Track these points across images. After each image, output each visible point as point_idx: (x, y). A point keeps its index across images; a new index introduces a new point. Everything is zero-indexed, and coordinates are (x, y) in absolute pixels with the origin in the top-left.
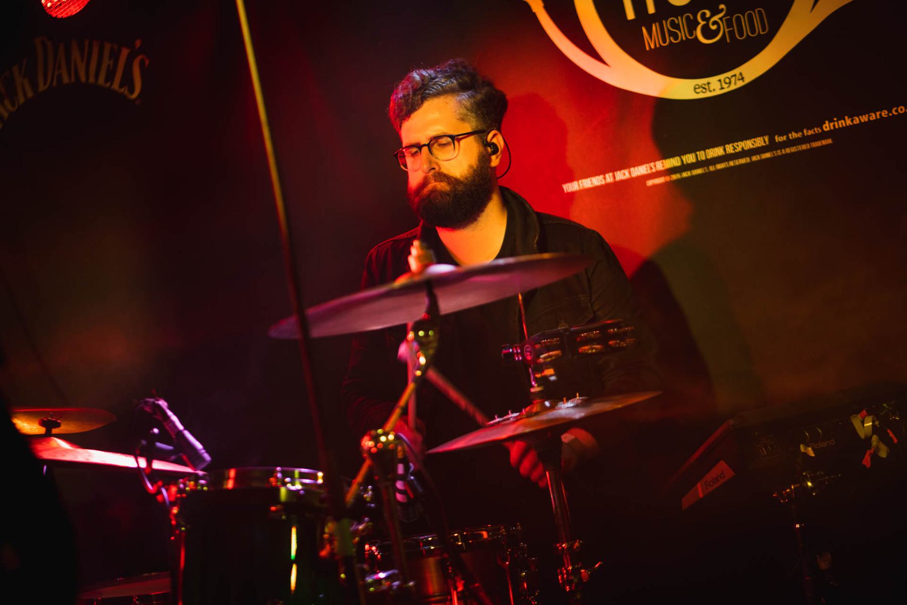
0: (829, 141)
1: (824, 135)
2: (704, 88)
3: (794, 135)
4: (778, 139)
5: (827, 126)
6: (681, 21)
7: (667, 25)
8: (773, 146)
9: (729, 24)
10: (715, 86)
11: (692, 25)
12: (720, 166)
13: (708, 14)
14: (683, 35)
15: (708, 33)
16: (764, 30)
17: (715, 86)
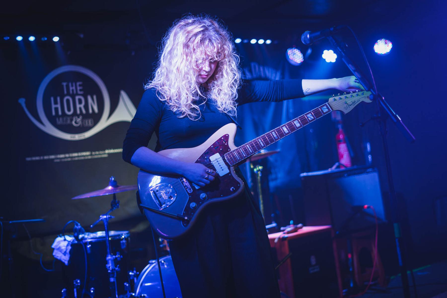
0: (106, 156)
1: (105, 154)
2: (74, 137)
3: (97, 153)
4: (93, 153)
5: (107, 151)
6: (69, 119)
7: (65, 119)
8: (91, 155)
9: (82, 120)
10: (77, 137)
11: (72, 120)
12: (76, 159)
13: (77, 117)
14: (69, 122)
15: (76, 122)
16: (92, 123)
17: (77, 137)
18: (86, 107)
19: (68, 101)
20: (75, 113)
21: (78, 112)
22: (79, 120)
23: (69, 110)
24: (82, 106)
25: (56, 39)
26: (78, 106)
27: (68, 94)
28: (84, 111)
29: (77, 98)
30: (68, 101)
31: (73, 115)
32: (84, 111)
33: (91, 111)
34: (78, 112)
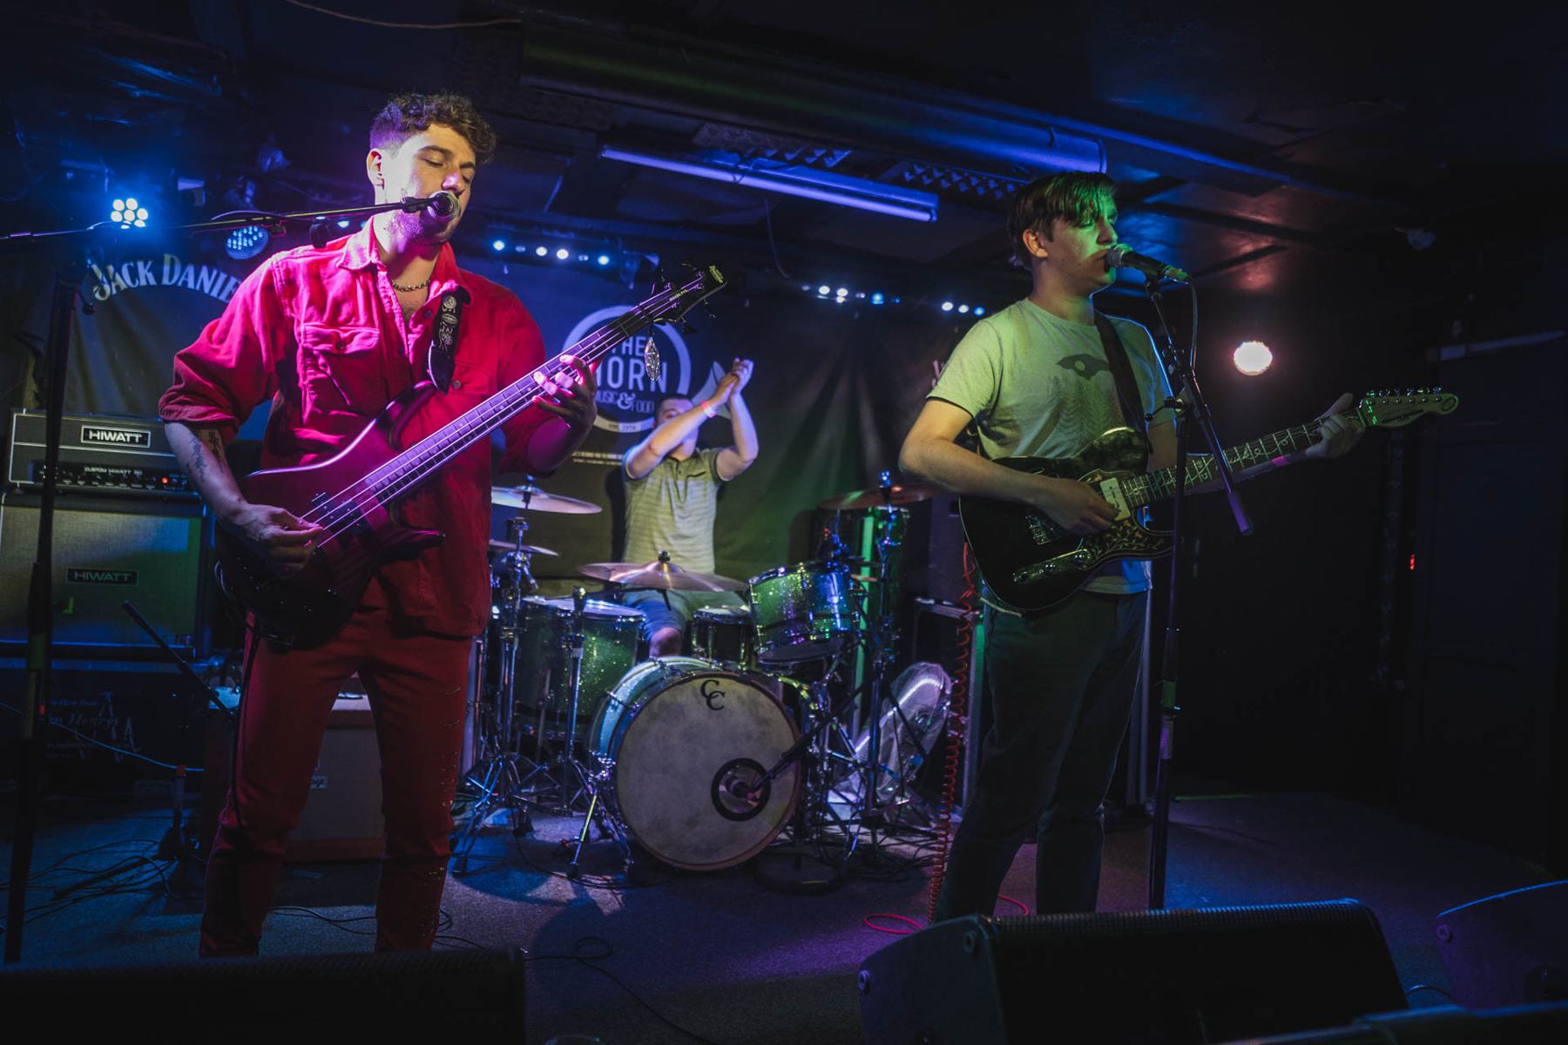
11: (617, 398)
14: (611, 400)
18: (646, 379)
19: (616, 365)
20: (624, 388)
21: (631, 386)
22: (629, 399)
23: (615, 380)
24: (639, 377)
25: (604, 260)
26: (632, 376)
27: (618, 353)
28: (641, 387)
29: (633, 362)
30: (616, 365)
31: (619, 390)
32: (641, 387)
33: (653, 388)
34: (631, 386)
